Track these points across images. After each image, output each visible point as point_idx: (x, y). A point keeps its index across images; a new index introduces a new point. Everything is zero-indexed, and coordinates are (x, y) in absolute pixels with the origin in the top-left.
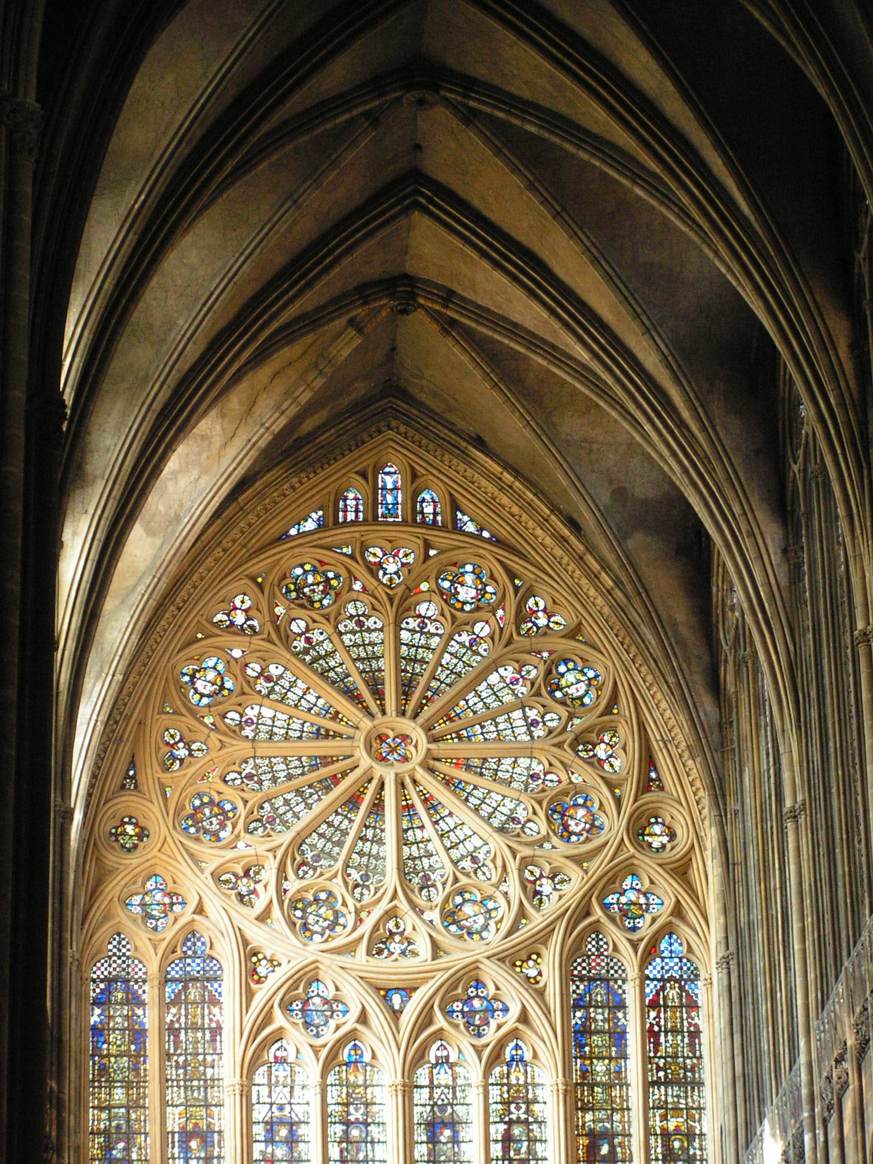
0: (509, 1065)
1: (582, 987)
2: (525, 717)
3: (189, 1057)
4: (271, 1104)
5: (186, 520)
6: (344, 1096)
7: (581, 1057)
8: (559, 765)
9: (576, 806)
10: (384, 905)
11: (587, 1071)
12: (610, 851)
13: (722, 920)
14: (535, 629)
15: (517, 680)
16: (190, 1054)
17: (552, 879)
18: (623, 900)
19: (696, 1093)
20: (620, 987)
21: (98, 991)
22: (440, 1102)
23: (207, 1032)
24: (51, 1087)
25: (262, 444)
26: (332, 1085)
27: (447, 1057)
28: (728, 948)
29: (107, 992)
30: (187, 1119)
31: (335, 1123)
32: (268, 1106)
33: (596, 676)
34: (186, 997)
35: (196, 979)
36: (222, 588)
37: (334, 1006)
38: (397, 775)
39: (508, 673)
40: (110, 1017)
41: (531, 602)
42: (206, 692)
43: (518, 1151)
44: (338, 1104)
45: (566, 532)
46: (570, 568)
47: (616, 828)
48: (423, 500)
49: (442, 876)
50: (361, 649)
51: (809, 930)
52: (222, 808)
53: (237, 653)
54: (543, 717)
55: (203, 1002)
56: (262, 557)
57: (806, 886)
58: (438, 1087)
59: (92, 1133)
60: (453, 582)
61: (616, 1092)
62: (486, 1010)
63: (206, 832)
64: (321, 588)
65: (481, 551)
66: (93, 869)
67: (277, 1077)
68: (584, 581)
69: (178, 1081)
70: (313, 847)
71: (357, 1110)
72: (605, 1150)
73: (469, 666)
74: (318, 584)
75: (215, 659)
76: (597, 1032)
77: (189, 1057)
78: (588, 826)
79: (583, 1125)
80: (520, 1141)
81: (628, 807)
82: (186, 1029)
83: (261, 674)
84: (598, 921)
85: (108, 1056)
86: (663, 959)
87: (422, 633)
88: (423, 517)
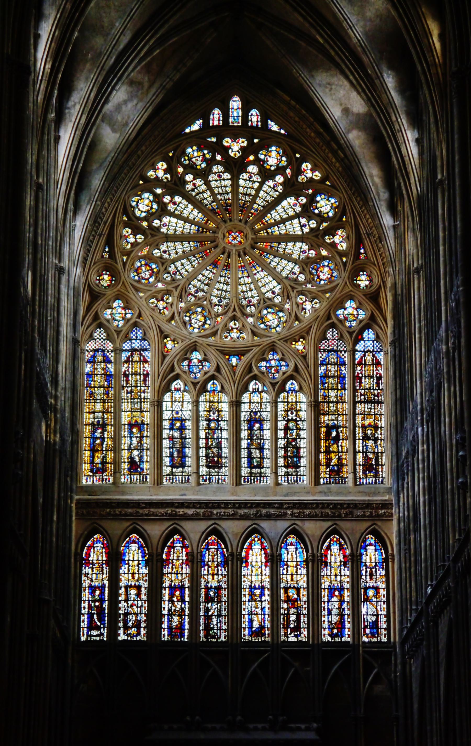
0: (288, 393)
1: (324, 355)
2: (300, 223)
4: (172, 411)
5: (131, 124)
6: (208, 407)
7: (323, 389)
8: (316, 246)
9: (324, 266)
10: (230, 314)
11: (326, 396)
12: (339, 288)
13: (392, 322)
14: (306, 179)
15: (296, 204)
17: (311, 302)
18: (346, 312)
19: (379, 407)
20: (343, 355)
21: (89, 356)
22: (254, 410)
23: (142, 376)
24: (51, 403)
25: (168, 86)
27: (258, 389)
28: (394, 336)
29: (94, 356)
33: (335, 202)
34: (132, 359)
35: (136, 350)
36: (152, 158)
37: (204, 364)
38: (236, 250)
39: (292, 200)
40: (96, 369)
41: (304, 166)
42: (144, 210)
43: (291, 435)
44: (205, 411)
45: (322, 130)
46: (324, 148)
47: (343, 276)
48: (252, 115)
49: (257, 300)
50: (220, 189)
51: (423, 328)
52: (151, 267)
53: (159, 191)
54: (308, 223)
55: (140, 361)
56: (172, 143)
57: (422, 306)
58: (254, 403)
59: (86, 425)
60: (265, 156)
61: (340, 406)
62: (277, 366)
63: (143, 278)
64: (201, 158)
65: (280, 140)
67: (175, 397)
68: (330, 155)
69: (127, 399)
70: (195, 286)
71: (214, 414)
72: (334, 434)
73: (273, 197)
74: (199, 157)
75: (148, 194)
76: (332, 377)
77: (133, 388)
78: (329, 276)
79: (324, 422)
80: (293, 430)
81: (349, 267)
82: (132, 374)
83: (171, 201)
84: (333, 323)
85: (94, 387)
86: (365, 341)
87: (250, 181)
88: (252, 123)
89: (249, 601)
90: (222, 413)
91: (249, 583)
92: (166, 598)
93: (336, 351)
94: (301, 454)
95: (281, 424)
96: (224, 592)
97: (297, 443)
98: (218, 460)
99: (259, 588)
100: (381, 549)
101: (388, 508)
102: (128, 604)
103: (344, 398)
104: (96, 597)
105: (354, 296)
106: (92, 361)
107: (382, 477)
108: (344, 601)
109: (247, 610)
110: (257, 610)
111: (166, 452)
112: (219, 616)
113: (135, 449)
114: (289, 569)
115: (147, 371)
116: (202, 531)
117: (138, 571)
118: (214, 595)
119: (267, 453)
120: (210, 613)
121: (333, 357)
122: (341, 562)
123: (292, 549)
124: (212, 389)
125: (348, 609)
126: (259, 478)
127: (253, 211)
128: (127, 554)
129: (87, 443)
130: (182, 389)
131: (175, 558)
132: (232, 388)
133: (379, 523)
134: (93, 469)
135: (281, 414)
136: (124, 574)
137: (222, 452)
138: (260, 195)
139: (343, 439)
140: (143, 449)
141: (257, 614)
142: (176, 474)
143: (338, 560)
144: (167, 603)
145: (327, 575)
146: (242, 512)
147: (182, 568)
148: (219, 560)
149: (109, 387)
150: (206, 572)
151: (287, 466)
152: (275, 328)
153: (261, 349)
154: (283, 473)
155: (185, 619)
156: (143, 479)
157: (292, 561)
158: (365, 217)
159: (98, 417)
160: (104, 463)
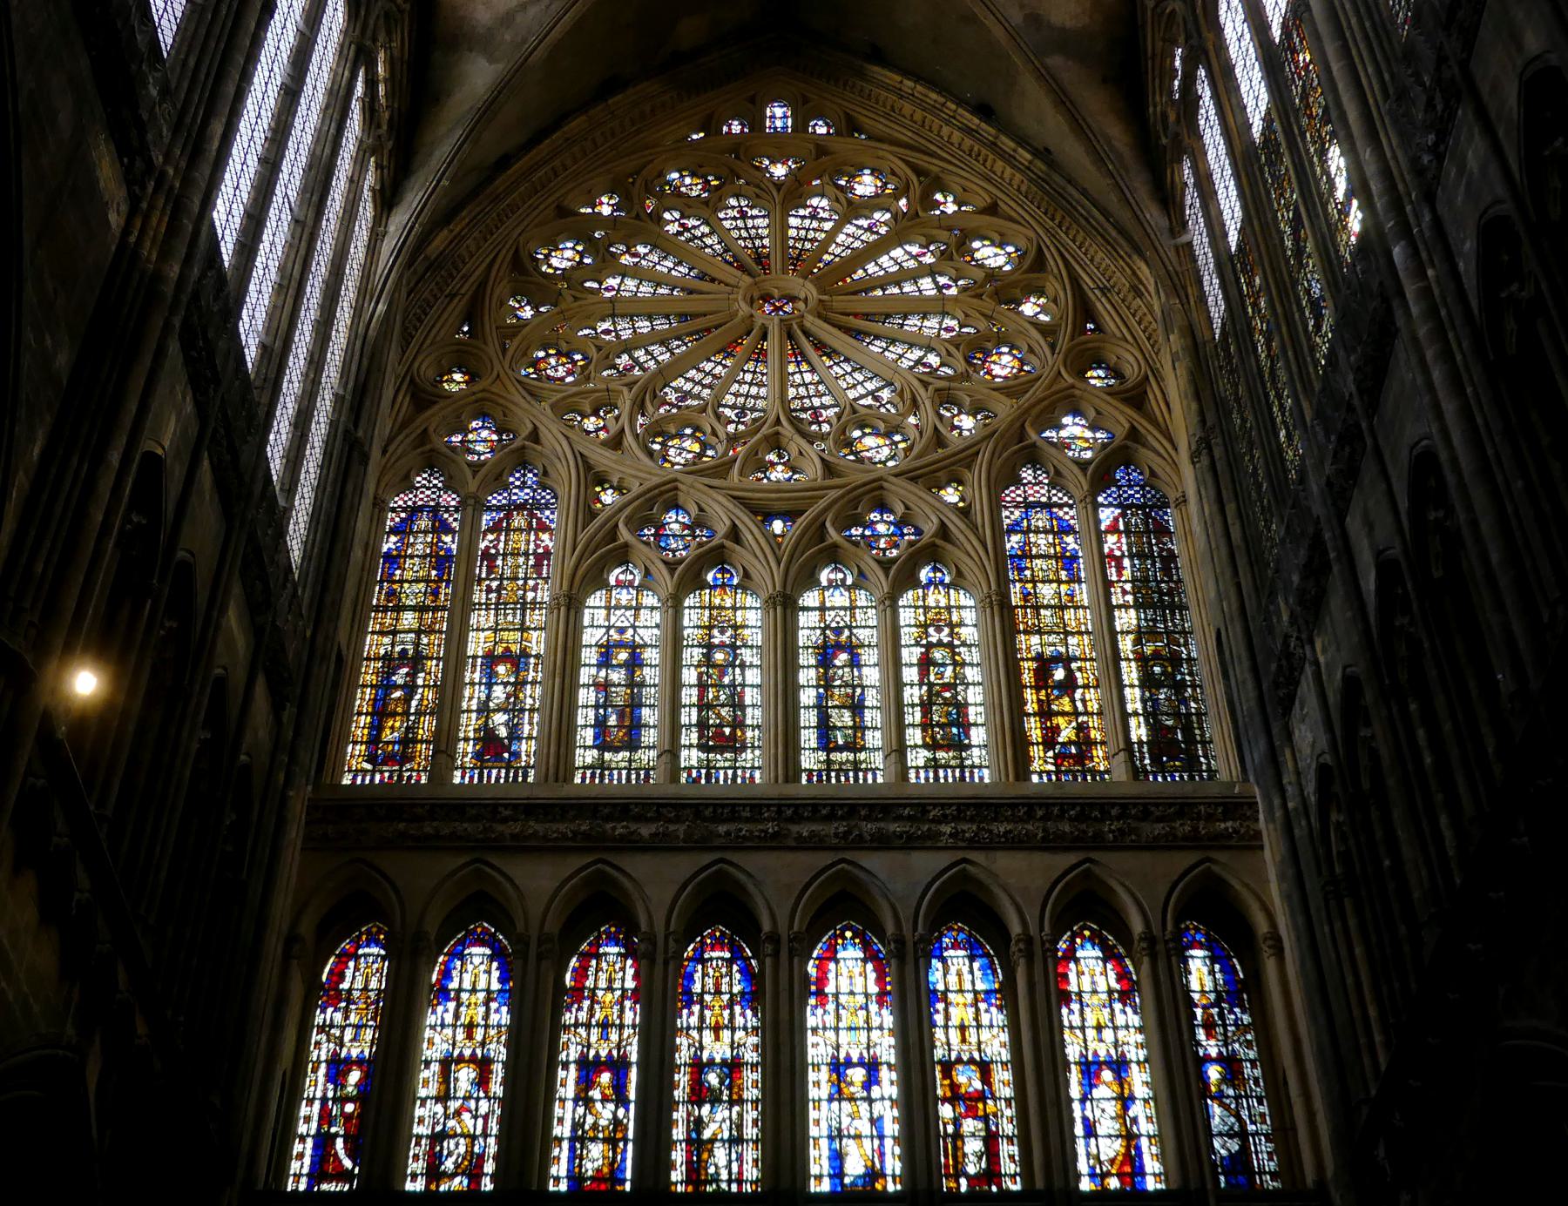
0: (926, 587)
3: (505, 582)
4: (609, 628)
6: (706, 619)
7: (1020, 580)
11: (1030, 594)
13: (1194, 406)
16: (508, 579)
21: (397, 520)
22: (834, 625)
26: (690, 608)
27: (844, 580)
30: (496, 643)
31: (693, 646)
32: (604, 630)
34: (509, 524)
35: (521, 507)
44: (698, 627)
52: (572, 359)
59: (368, 659)
61: (1069, 615)
62: (893, 534)
65: (881, 153)
66: (406, 404)
68: (1000, 164)
70: (677, 390)
71: (722, 632)
72: (1059, 674)
77: (505, 582)
80: (944, 665)
82: (505, 555)
85: (401, 582)
86: (1119, 488)
89: (831, 1099)
90: (746, 632)
91: (830, 1051)
92: (569, 1091)
93: (1048, 506)
94: (972, 719)
95: (911, 655)
96: (750, 1077)
97: (957, 693)
98: (733, 733)
99: (861, 1063)
100: (1230, 958)
101: (1244, 818)
102: (446, 1108)
103: (1078, 598)
104: (350, 1089)
105: (1081, 398)
106: (401, 530)
107: (1209, 770)
108: (1132, 1098)
109: (824, 1125)
110: (856, 1123)
111: (586, 716)
112: (736, 1140)
113: (498, 710)
114: (951, 1009)
115: (546, 548)
116: (682, 880)
117: (486, 1016)
118: (722, 1083)
119: (872, 717)
120: (707, 1134)
121: (1040, 519)
122: (1110, 992)
123: (957, 958)
124: (719, 583)
125: (1149, 1119)
126: (851, 774)
127: (821, 265)
128: (455, 973)
129: (367, 697)
130: (636, 584)
131: (603, 984)
132: (768, 575)
133: (1222, 856)
134: (377, 756)
135: (908, 635)
136: (443, 1026)
137: (744, 715)
138: (839, 240)
139: (1086, 686)
140: (522, 710)
141: (858, 1137)
142: (614, 765)
143: (1102, 987)
144: (569, 1105)
145: (1071, 1027)
146: (805, 830)
147: (622, 1011)
148: (736, 989)
149: (440, 580)
150: (694, 1021)
151: (933, 746)
152: (884, 463)
153: (849, 492)
154: (921, 763)
155: (625, 1151)
156: (516, 776)
157: (961, 991)
158: (1092, 260)
159: (403, 643)
160: (408, 740)
